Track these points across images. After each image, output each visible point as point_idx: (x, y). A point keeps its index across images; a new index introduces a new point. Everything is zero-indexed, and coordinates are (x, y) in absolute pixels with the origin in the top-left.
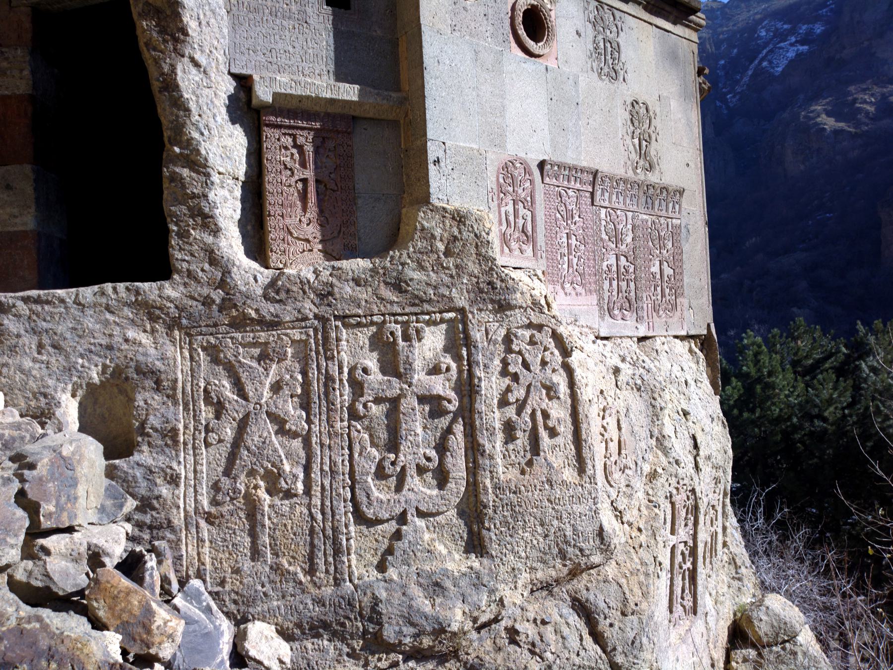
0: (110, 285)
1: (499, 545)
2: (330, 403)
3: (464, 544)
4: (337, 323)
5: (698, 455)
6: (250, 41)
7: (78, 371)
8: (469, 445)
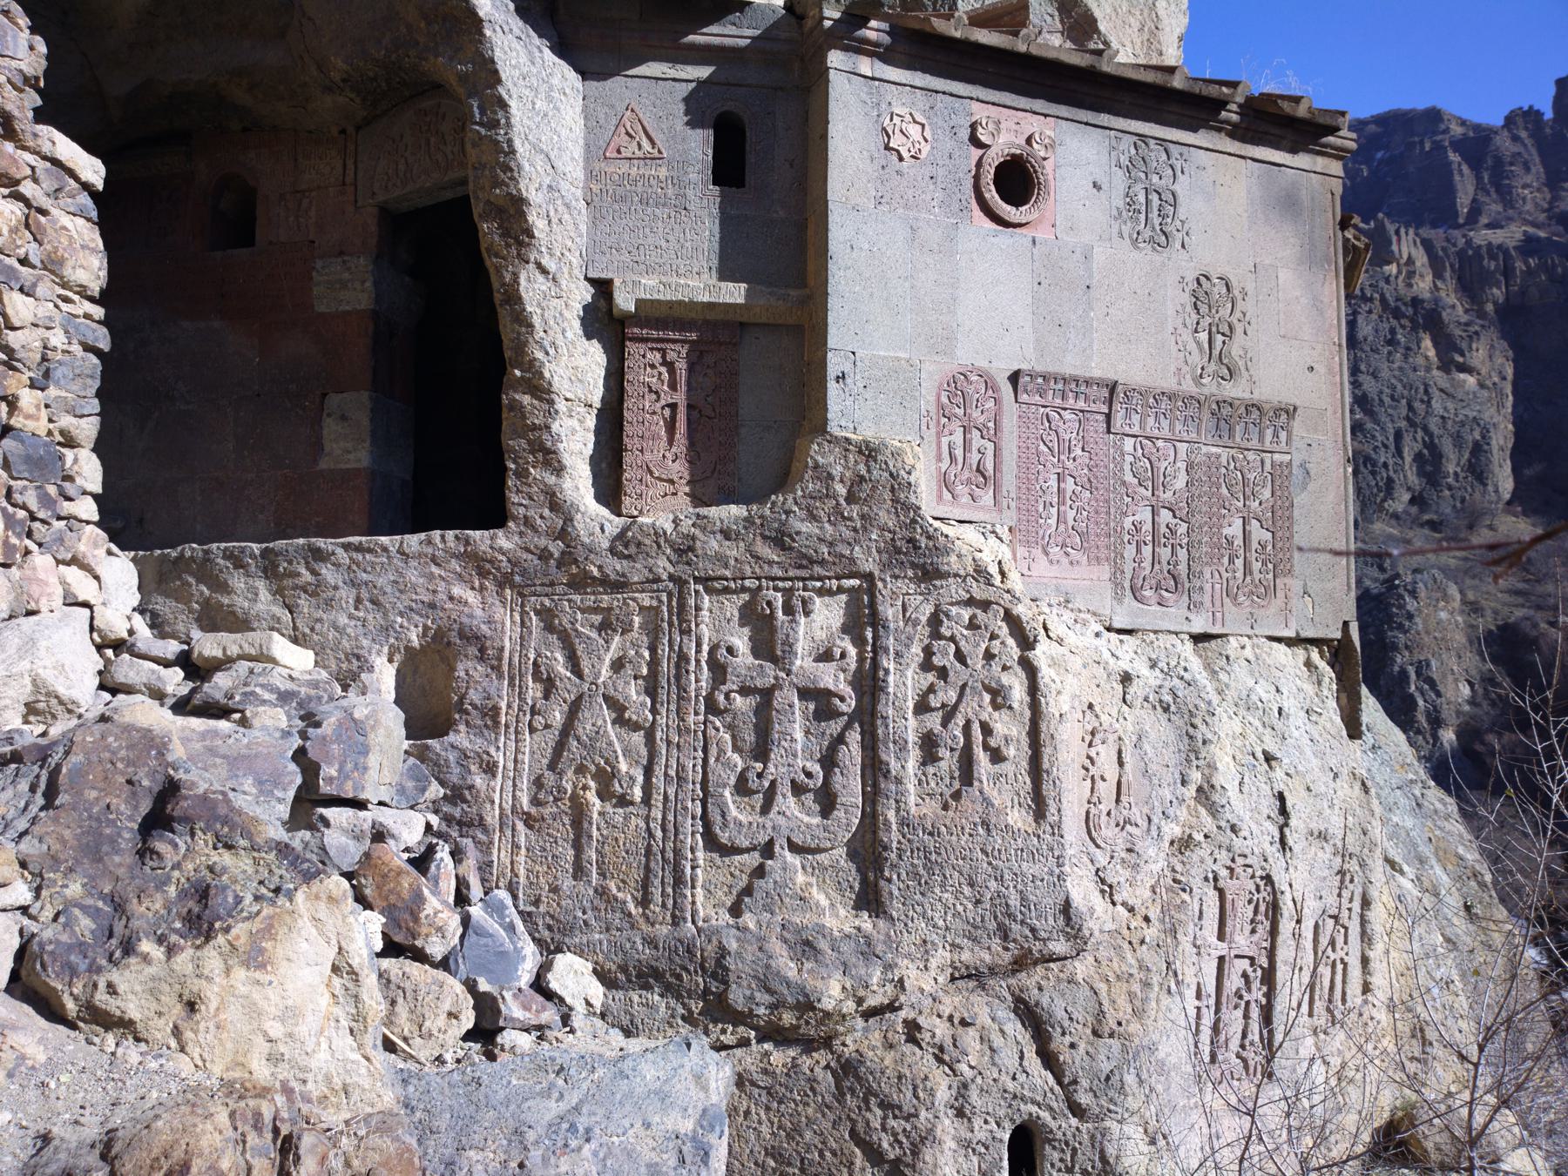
0: (439, 532)
2: (682, 689)
5: (1287, 825)
6: (614, 238)
8: (867, 762)
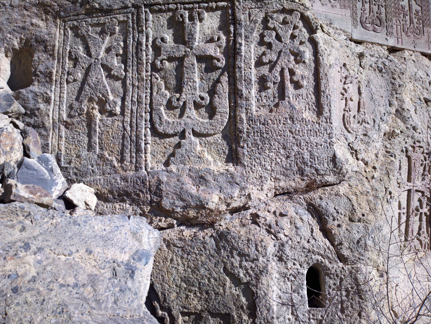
1: (250, 159)
2: (139, 59)
3: (225, 157)
4: (146, 9)
7: (7, 41)
8: (231, 91)
